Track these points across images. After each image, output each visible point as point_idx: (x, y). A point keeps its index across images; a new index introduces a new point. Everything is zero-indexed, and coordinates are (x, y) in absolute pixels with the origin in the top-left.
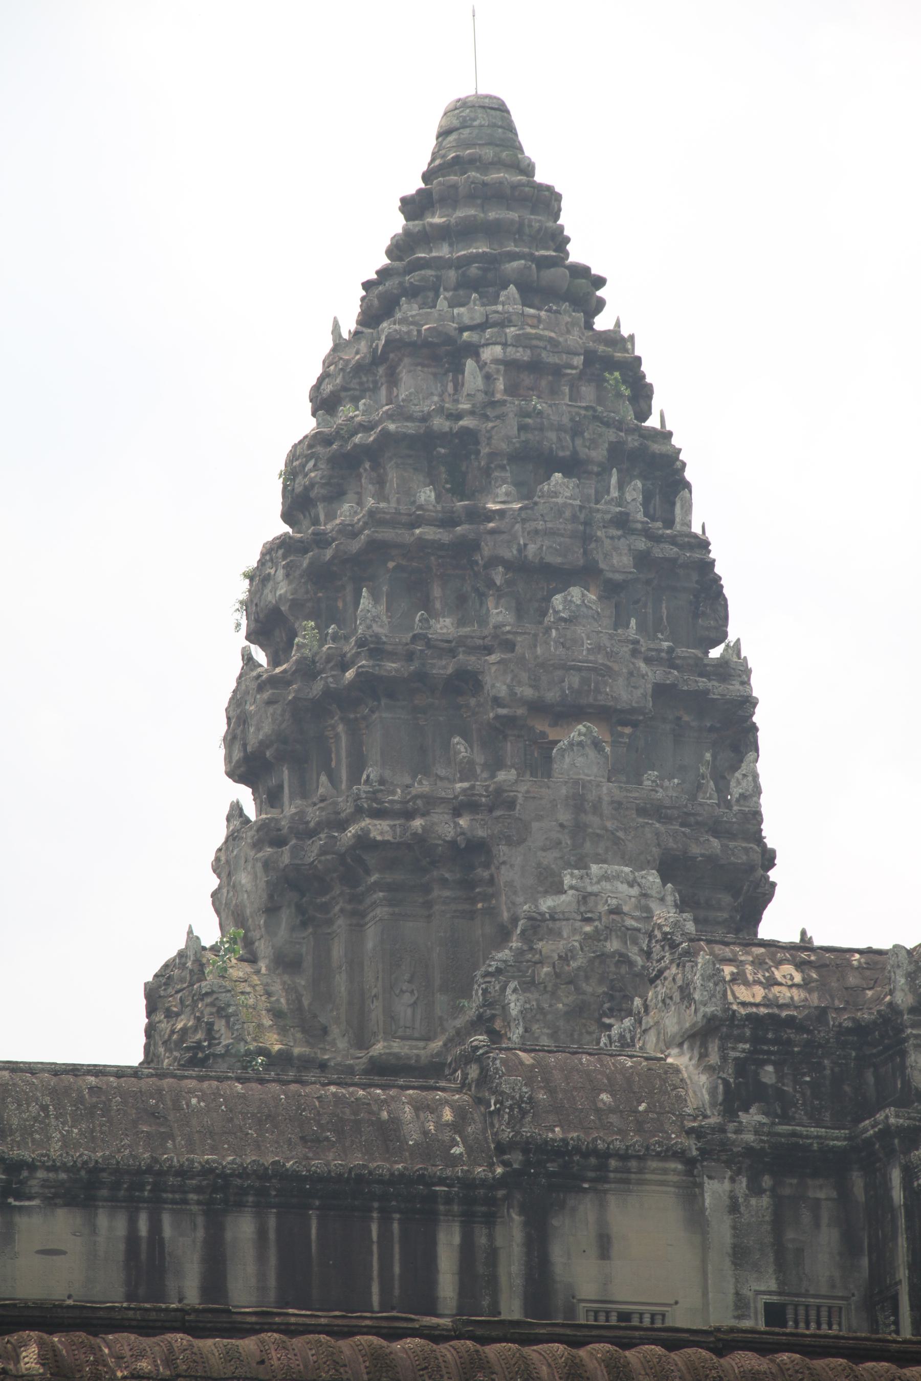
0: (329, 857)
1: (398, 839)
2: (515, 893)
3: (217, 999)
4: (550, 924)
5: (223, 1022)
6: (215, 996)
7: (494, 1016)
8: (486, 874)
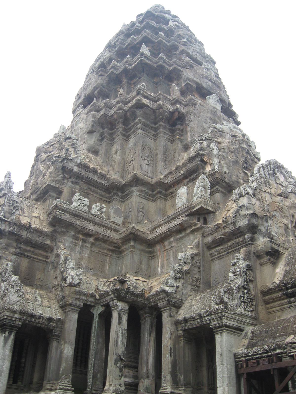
0: (121, 111)
1: (151, 107)
2: (195, 132)
3: (72, 141)
5: (73, 149)
8: (181, 128)
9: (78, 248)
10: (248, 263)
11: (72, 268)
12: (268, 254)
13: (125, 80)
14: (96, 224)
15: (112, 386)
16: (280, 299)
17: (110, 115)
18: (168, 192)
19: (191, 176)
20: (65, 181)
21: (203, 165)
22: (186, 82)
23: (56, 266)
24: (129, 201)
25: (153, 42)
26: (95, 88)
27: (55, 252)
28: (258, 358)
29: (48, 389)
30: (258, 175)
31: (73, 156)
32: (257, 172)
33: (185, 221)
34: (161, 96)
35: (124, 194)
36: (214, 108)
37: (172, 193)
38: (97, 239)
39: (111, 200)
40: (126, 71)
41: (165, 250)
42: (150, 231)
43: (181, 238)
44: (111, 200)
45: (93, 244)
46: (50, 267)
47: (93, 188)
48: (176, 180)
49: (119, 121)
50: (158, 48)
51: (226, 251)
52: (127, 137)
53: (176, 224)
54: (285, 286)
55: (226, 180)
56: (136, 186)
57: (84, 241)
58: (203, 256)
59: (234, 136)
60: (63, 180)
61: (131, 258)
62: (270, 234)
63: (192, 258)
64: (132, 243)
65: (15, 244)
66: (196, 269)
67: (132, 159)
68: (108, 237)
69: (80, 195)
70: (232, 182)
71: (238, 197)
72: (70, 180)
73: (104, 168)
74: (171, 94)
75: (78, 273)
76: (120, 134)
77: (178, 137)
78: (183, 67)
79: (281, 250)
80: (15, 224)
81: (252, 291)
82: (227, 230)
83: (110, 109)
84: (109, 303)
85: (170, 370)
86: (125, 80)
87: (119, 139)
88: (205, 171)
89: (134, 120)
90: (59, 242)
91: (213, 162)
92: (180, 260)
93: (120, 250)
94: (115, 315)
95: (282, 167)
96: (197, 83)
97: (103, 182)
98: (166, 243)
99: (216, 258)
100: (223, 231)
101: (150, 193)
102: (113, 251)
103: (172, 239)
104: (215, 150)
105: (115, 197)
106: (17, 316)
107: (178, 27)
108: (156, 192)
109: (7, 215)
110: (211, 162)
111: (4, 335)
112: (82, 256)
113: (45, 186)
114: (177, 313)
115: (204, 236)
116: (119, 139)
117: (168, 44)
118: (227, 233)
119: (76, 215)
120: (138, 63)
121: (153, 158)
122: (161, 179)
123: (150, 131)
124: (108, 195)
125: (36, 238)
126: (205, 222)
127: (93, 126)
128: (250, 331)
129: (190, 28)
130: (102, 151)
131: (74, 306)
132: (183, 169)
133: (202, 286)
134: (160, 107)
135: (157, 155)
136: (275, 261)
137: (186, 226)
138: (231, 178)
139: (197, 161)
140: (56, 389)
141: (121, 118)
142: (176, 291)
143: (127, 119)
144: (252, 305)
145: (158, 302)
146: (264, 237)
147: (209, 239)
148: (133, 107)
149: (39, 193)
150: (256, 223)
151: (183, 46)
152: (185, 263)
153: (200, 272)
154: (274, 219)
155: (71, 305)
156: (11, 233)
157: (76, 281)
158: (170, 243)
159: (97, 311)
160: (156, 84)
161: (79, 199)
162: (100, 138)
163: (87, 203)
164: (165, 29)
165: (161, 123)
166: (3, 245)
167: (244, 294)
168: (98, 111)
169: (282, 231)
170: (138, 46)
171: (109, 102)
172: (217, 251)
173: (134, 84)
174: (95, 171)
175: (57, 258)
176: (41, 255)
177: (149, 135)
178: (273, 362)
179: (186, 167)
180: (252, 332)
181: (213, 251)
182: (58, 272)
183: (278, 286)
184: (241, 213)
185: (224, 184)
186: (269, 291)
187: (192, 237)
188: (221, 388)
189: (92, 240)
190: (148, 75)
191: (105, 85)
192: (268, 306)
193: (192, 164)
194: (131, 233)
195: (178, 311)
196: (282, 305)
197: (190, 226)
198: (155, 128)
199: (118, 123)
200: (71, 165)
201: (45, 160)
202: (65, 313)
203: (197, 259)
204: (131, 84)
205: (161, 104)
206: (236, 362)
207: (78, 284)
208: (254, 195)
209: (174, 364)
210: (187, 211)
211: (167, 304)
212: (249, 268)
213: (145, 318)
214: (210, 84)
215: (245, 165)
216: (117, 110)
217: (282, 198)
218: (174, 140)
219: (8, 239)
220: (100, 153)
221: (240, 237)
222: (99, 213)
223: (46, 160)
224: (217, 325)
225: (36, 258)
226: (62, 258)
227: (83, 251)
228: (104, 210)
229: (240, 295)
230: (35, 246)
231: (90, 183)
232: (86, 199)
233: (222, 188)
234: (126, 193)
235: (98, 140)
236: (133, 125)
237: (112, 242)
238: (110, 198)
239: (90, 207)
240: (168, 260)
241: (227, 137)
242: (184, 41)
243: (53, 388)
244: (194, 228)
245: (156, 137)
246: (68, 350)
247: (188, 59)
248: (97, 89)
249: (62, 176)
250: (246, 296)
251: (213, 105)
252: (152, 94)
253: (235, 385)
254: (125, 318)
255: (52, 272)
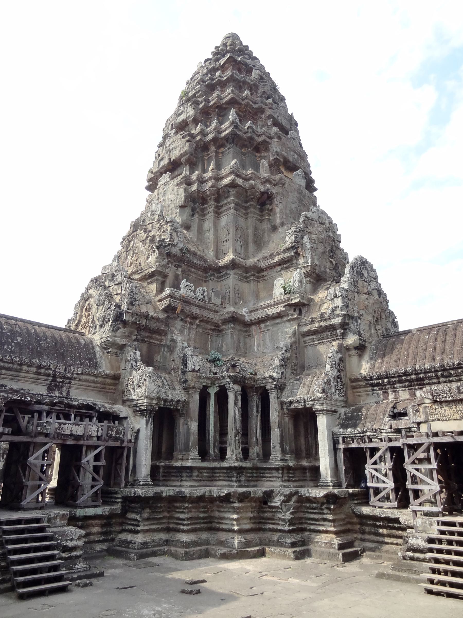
0: (214, 189)
1: (244, 187)
4: (311, 222)
5: (175, 234)
6: (173, 223)
7: (299, 247)
8: (270, 208)
9: (186, 330)
10: (340, 356)
11: (192, 356)
12: (356, 348)
13: (213, 148)
14: (200, 307)
15: (234, 455)
16: (365, 386)
17: (203, 190)
18: (260, 275)
19: (284, 264)
20: (170, 265)
21: (297, 256)
22: (275, 157)
23: (171, 349)
24: (224, 283)
25: (239, 104)
26: (182, 155)
27: (169, 337)
28: (353, 437)
29: (180, 459)
30: (348, 275)
31: (175, 241)
32: (348, 272)
33: (283, 311)
34: (253, 175)
35: (219, 275)
36: (300, 186)
37: (264, 276)
38: (200, 321)
39: (207, 279)
40: (215, 140)
41: (261, 332)
42: (247, 313)
43: (278, 323)
44: (207, 279)
45: (198, 326)
46: (166, 350)
47: (193, 270)
48: (269, 266)
49: (211, 198)
50: (244, 110)
51: (318, 340)
52: (218, 214)
53: (274, 312)
54: (371, 377)
55: (317, 272)
56: (233, 269)
57: (191, 323)
58: (299, 344)
59: (322, 224)
60: (168, 264)
61: (231, 338)
62: (359, 332)
63: (291, 346)
64: (232, 325)
65: (136, 332)
66: (294, 355)
67: (225, 239)
68: (211, 319)
69: (187, 282)
70: (321, 272)
71: (333, 297)
72: (174, 264)
73: (200, 247)
74: (261, 171)
75: (198, 360)
76: (212, 212)
77: (267, 217)
78: (271, 138)
79: (367, 344)
80: (137, 314)
81: (343, 379)
82: (321, 324)
83: (203, 184)
84: (225, 385)
85: (279, 442)
86: (213, 148)
87: (210, 216)
88: (298, 263)
89: (228, 197)
90: (172, 326)
91: (307, 255)
92: (282, 348)
93: (220, 329)
94: (231, 397)
95: (367, 262)
96: (285, 158)
97: (201, 264)
98: (262, 325)
99: (310, 345)
100: (317, 325)
101: (245, 275)
102: (213, 330)
103: (269, 323)
104: (308, 244)
105: (212, 277)
106: (155, 402)
107: (262, 78)
108: (250, 274)
109: (130, 307)
110: (304, 255)
111: (145, 418)
112: (190, 338)
113: (151, 270)
114: (282, 394)
115: (299, 325)
116: (210, 216)
117: (255, 106)
118: (321, 326)
119: (186, 301)
120: (228, 134)
121: (245, 239)
122: (256, 263)
123: (242, 210)
124: (205, 275)
125: (154, 325)
126: (300, 314)
127: (185, 201)
128: (343, 414)
129: (271, 76)
130: (195, 227)
131: (196, 389)
132: (276, 257)
133: (298, 369)
134: (253, 187)
135: (248, 235)
136: (361, 353)
137: (283, 314)
138: (320, 269)
139: (292, 253)
140: (188, 459)
141: (214, 195)
142: (281, 377)
143: (219, 195)
144: (343, 390)
145: (265, 385)
146: (354, 334)
147: (305, 329)
148: (226, 186)
149: (143, 274)
150: (347, 321)
151: (270, 110)
152: (286, 351)
153: (297, 357)
154: (362, 317)
155: (193, 388)
156: (134, 323)
157: (197, 368)
158: (266, 326)
159: (213, 391)
160: (244, 154)
161: (187, 286)
162: (191, 213)
163: (193, 289)
164: (249, 83)
165: (252, 203)
166: (127, 333)
167: (338, 382)
168: (189, 183)
169: (367, 328)
170: (224, 106)
171: (201, 176)
172: (310, 339)
173: (222, 153)
174: (195, 254)
175: (172, 342)
176: (157, 339)
177: (241, 214)
178: (365, 442)
179: (280, 256)
180: (345, 414)
181: (307, 338)
182: (175, 356)
183: (365, 377)
184: (335, 312)
185: (315, 275)
186: (357, 380)
187: (288, 324)
188: (324, 459)
189: (197, 322)
190: (236, 145)
191: (193, 152)
192: (354, 390)
193: (286, 254)
194: (233, 317)
195: (282, 393)
196: (367, 391)
197: (287, 315)
198: (246, 207)
199: (210, 199)
200: (175, 250)
201: (145, 240)
202: (188, 394)
203: (294, 346)
204: (219, 153)
205: (254, 184)
206: (333, 438)
207: (199, 370)
208: (346, 297)
209: (282, 437)
210: (285, 302)
211: (275, 388)
212: (341, 360)
213: (253, 395)
214: (296, 156)
215: (331, 254)
216: (210, 187)
217: (367, 296)
218: (263, 220)
219: (131, 327)
220: (192, 228)
221: (333, 331)
222: (202, 297)
223: (148, 241)
224: (319, 409)
225: (153, 343)
226: (179, 345)
227: (190, 333)
228: (206, 293)
229: (335, 384)
230: (152, 331)
231: (191, 264)
232: (192, 284)
233: (312, 278)
234: (222, 274)
235: (189, 215)
236: (226, 204)
237: (213, 323)
238: (206, 277)
239: (195, 292)
240: (264, 341)
241: (316, 226)
242: (270, 103)
243: (184, 458)
244: (290, 317)
245: (246, 216)
246: (194, 426)
247: (275, 129)
248: (184, 156)
249: (166, 260)
250: (339, 384)
251: (299, 182)
252: (244, 172)
253: (333, 456)
254: (239, 398)
255: (168, 355)
